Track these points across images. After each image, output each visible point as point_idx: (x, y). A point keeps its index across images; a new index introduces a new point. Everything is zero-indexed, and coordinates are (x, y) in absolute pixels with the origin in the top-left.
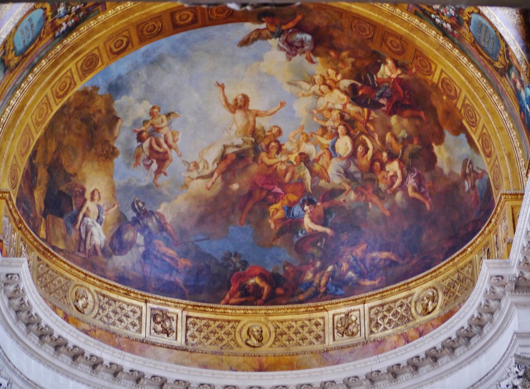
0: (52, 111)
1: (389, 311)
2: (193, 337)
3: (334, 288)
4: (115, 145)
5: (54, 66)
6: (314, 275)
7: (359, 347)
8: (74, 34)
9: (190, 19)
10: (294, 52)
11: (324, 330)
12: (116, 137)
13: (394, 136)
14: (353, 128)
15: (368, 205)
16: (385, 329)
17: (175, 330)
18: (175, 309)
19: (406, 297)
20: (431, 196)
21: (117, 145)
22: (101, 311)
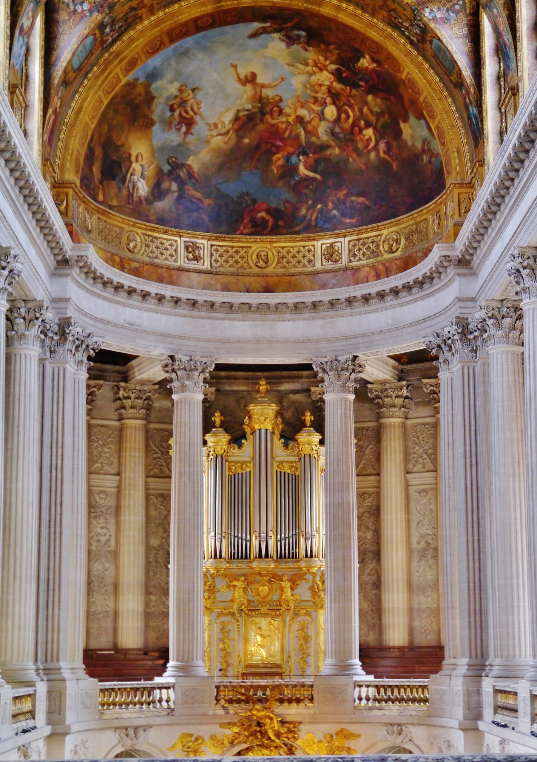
0: (103, 104)
1: (364, 244)
2: (216, 261)
3: (322, 223)
4: (153, 117)
5: (103, 71)
6: (307, 212)
7: (341, 272)
8: (118, 43)
9: (209, 23)
11: (314, 256)
12: (153, 111)
15: (349, 159)
16: (360, 259)
17: (202, 256)
19: (377, 236)
20: (397, 159)
21: (155, 117)
22: (147, 249)
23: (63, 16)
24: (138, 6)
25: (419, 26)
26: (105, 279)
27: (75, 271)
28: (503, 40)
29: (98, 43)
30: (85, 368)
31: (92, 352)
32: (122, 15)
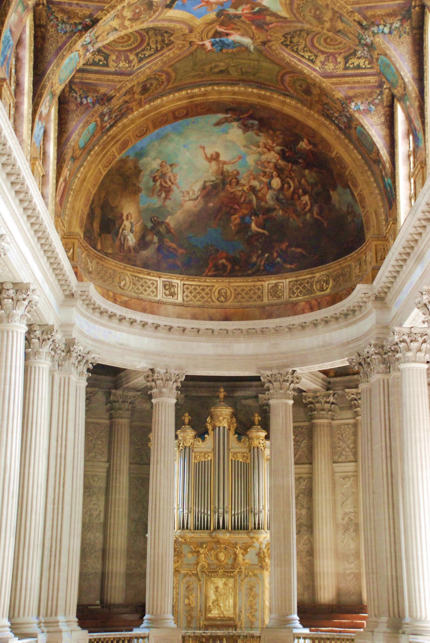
1: (300, 285)
2: (187, 296)
11: (262, 293)
13: (306, 180)
16: (298, 296)
18: (177, 281)
19: (310, 278)
21: (141, 186)
23: (72, 106)
25: (346, 116)
26: (102, 309)
29: (98, 128)
30: (85, 378)
32: (118, 107)
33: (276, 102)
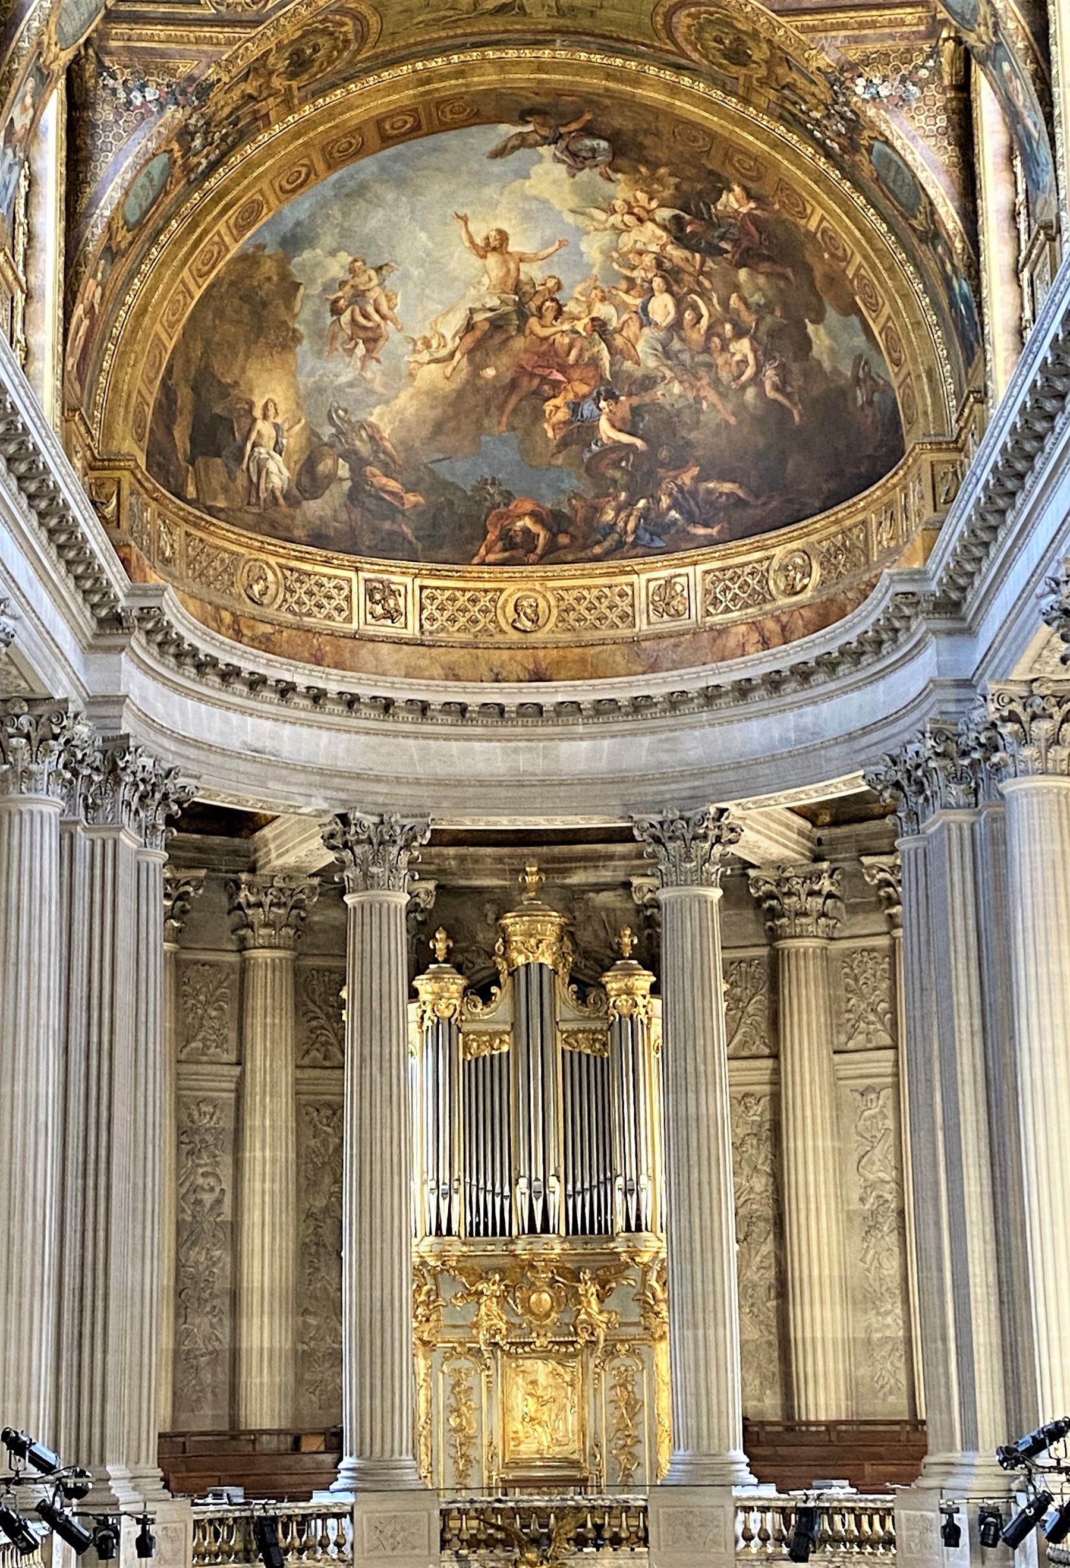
2: (432, 619)
3: (648, 536)
4: (297, 326)
5: (191, 229)
6: (617, 515)
9: (408, 126)
10: (580, 166)
11: (632, 606)
13: (743, 299)
14: (677, 282)
16: (727, 610)
18: (404, 579)
19: (759, 561)
22: (288, 595)
23: (104, 113)
24: (260, 93)
25: (843, 117)
27: (137, 640)
28: (1025, 127)
29: (177, 171)
30: (160, 841)
31: (175, 807)
32: (227, 111)
33: (654, 87)
